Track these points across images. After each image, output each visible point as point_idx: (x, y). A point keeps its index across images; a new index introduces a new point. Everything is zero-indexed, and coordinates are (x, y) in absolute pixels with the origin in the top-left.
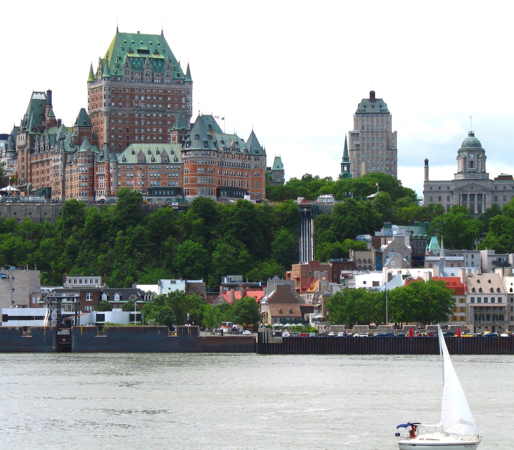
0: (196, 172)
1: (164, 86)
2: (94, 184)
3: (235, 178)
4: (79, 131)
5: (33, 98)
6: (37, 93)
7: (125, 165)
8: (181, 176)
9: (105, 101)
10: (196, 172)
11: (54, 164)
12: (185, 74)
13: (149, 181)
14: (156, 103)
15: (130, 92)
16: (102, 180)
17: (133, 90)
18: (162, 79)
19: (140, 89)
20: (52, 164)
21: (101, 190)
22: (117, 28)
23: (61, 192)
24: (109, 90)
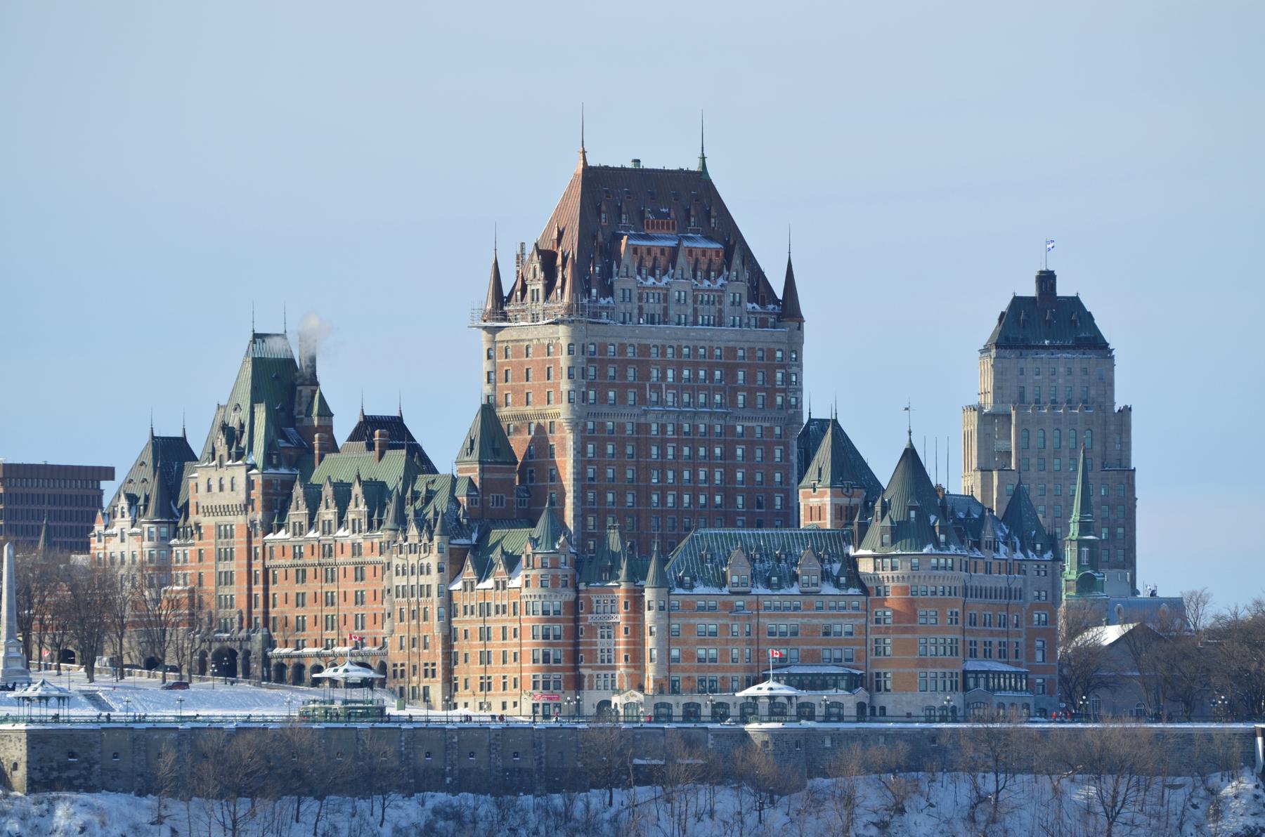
0: (915, 621)
2: (576, 652)
3: (992, 633)
4: (482, 479)
7: (694, 598)
8: (860, 633)
11: (400, 581)
12: (780, 296)
14: (707, 388)
16: (606, 640)
17: (644, 350)
18: (720, 311)
20: (390, 578)
21: (603, 672)
23: (439, 669)
24: (583, 354)
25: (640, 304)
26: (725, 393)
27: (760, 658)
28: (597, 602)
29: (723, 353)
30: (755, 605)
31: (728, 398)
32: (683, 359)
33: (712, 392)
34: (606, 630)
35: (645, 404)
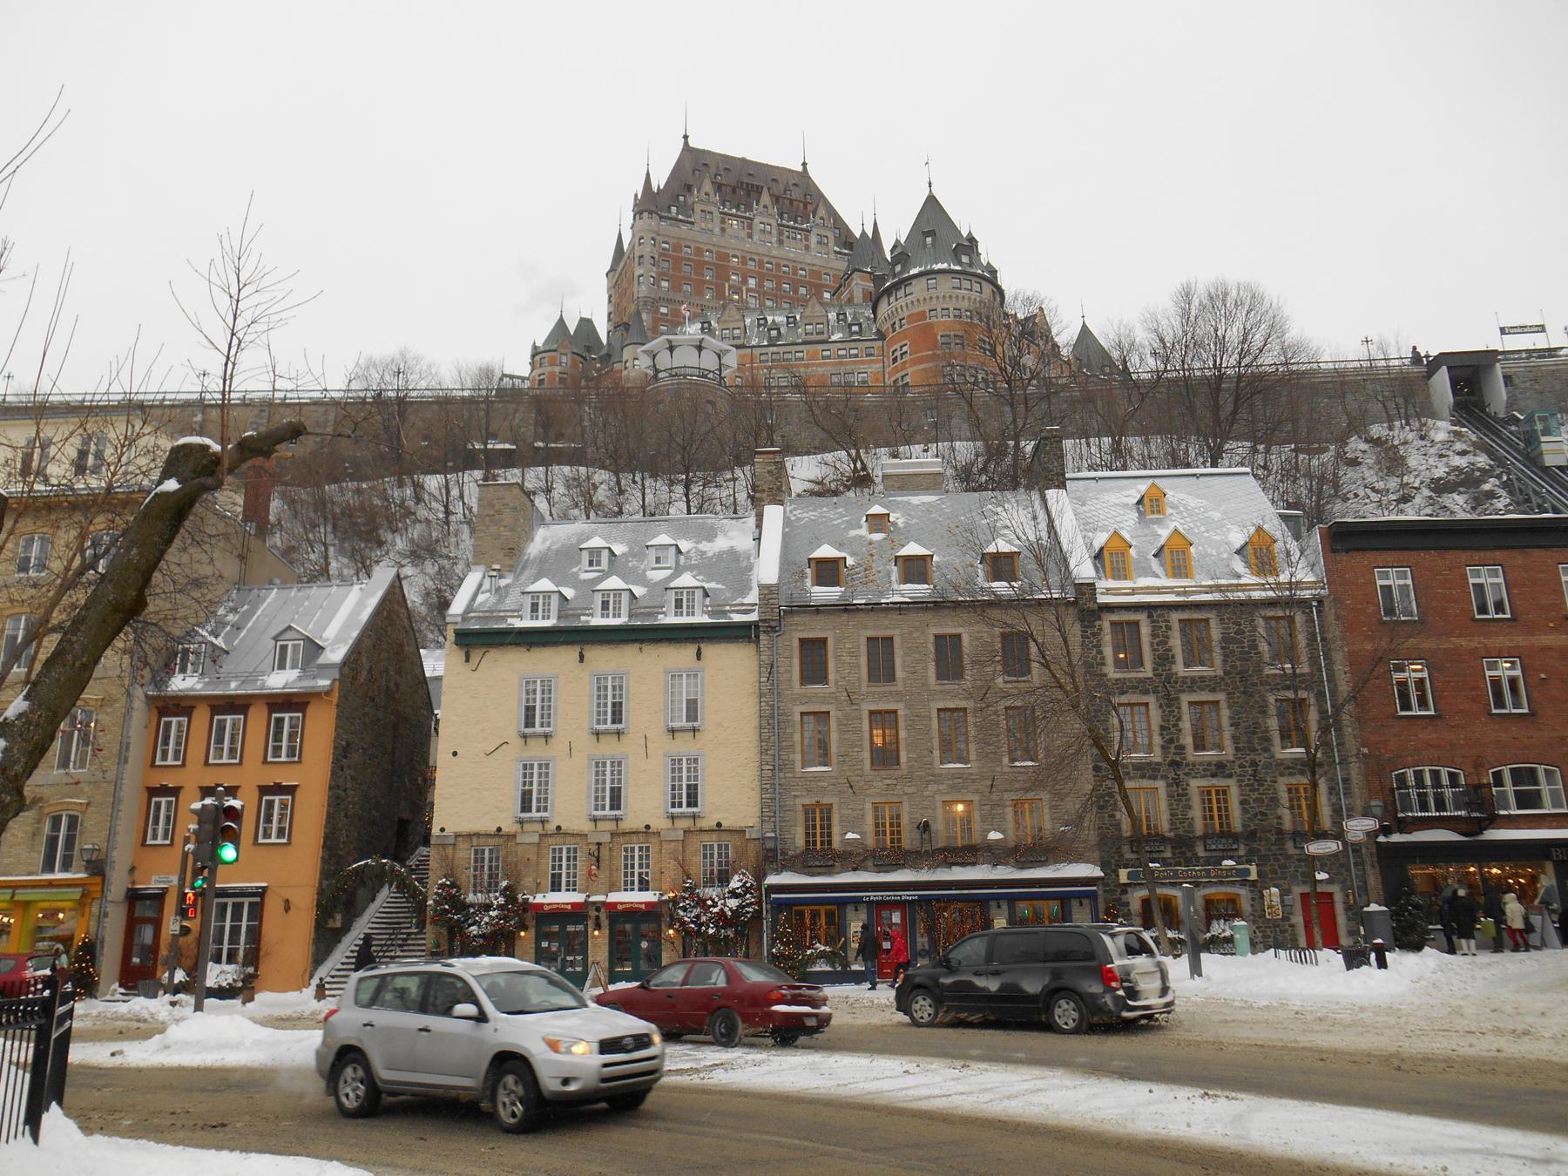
1: (808, 259)
8: (877, 380)
9: (641, 272)
15: (715, 261)
19: (744, 257)
22: (686, 137)
32: (765, 271)
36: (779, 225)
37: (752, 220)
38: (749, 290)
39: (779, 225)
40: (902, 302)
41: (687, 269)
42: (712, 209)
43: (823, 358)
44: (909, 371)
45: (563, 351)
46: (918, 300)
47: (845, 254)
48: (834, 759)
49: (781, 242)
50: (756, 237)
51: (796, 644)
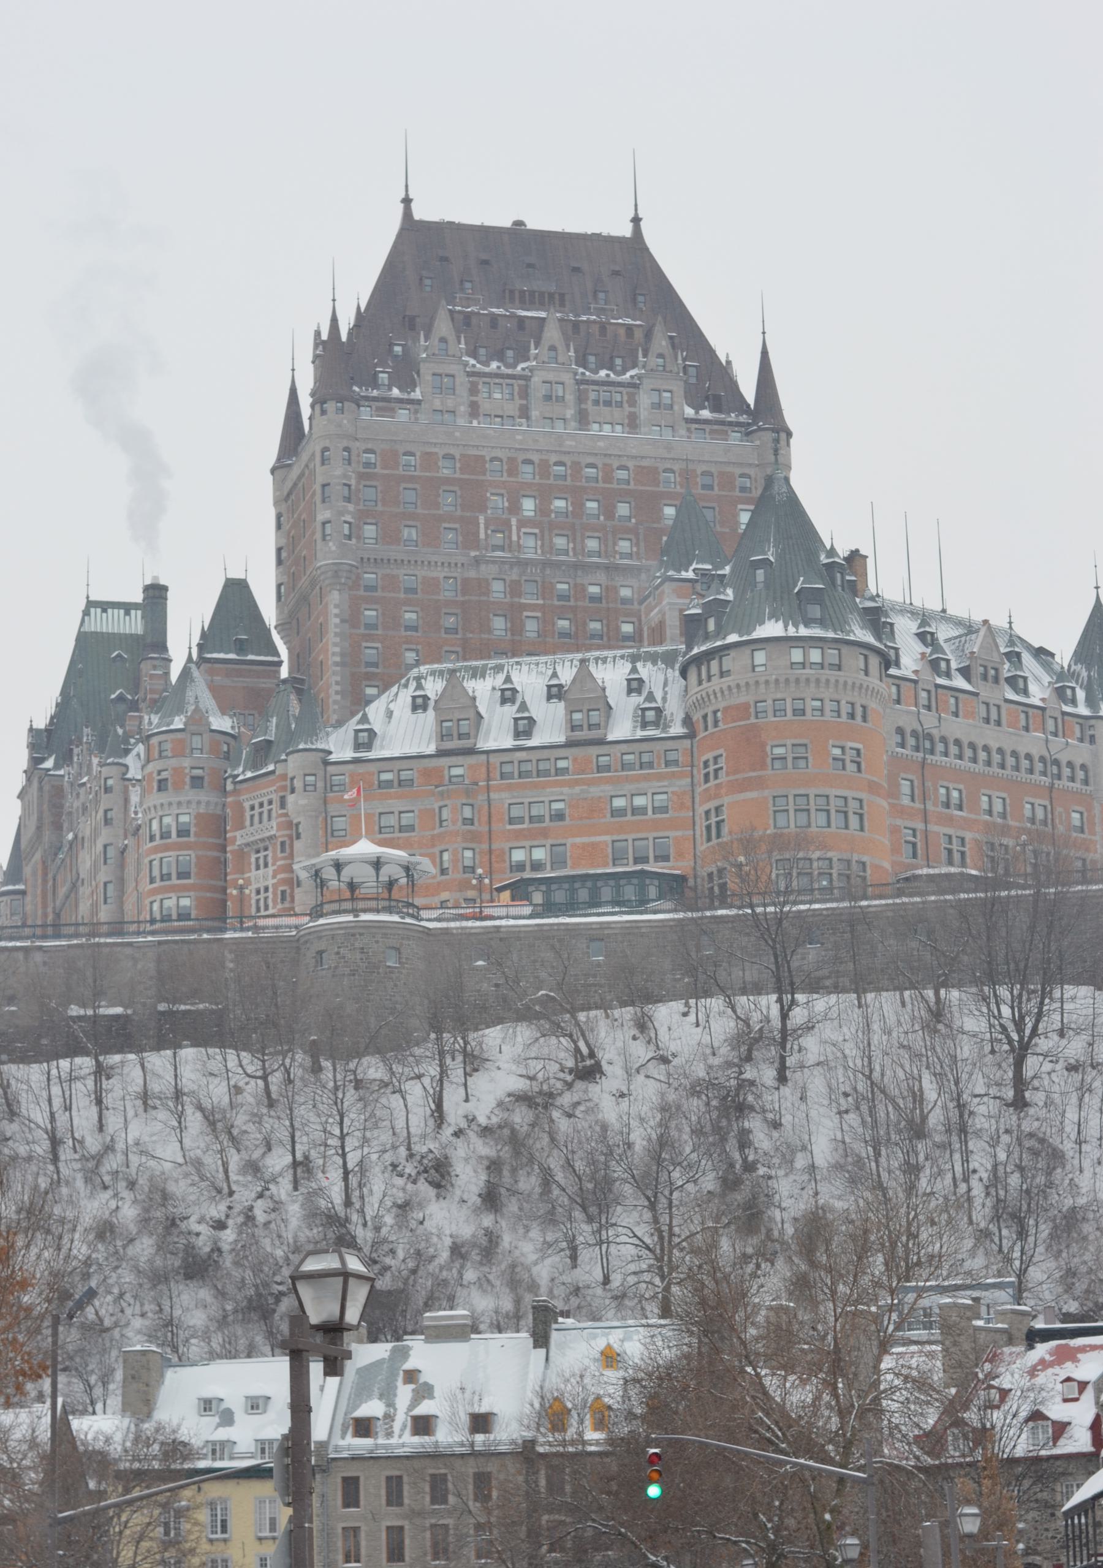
0: (763, 766)
2: (223, 903)
5: (86, 628)
6: (105, 606)
7: (372, 768)
10: (763, 766)
13: (506, 846)
15: (457, 476)
16: (261, 871)
17: (474, 464)
22: (407, 201)
25: (474, 399)
26: (637, 535)
27: (495, 865)
28: (252, 808)
29: (632, 476)
30: (484, 770)
31: (642, 544)
32: (551, 481)
33: (610, 536)
34: (262, 855)
35: (477, 547)
36: (579, 383)
37: (527, 379)
38: (523, 523)
39: (579, 383)
40: (716, 683)
41: (410, 496)
42: (453, 369)
43: (599, 769)
44: (726, 800)
45: (193, 728)
46: (738, 686)
47: (706, 422)
48: (363, 1558)
49: (583, 419)
50: (535, 414)
51: (339, 1480)
